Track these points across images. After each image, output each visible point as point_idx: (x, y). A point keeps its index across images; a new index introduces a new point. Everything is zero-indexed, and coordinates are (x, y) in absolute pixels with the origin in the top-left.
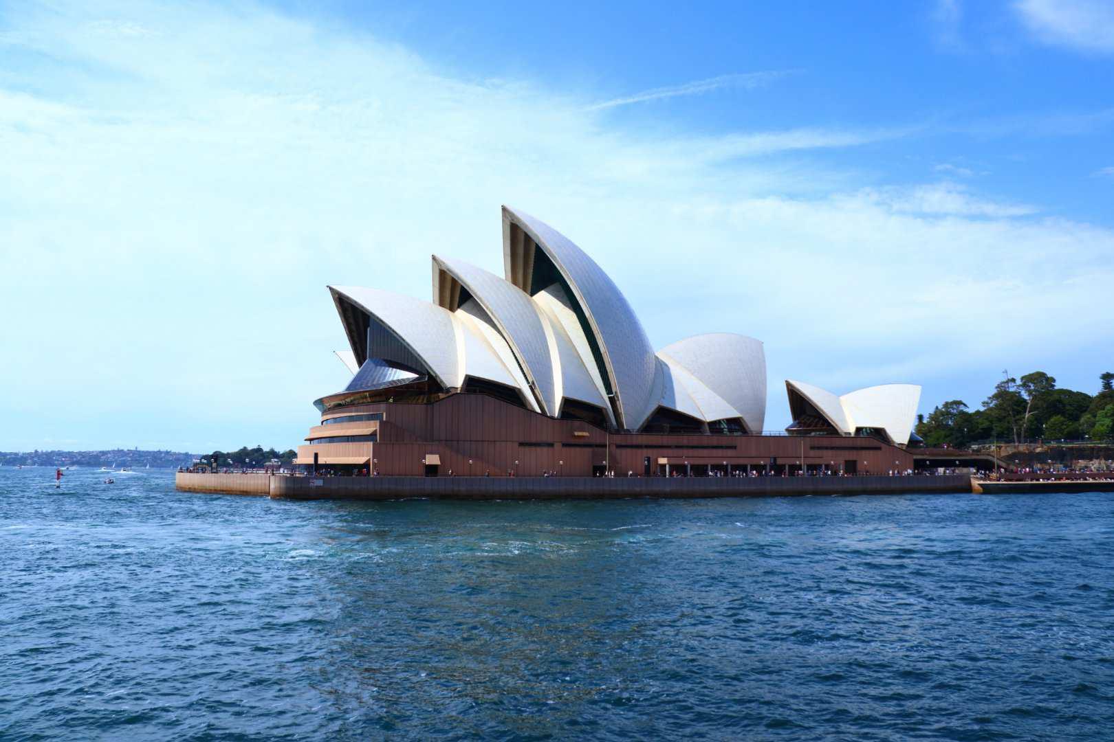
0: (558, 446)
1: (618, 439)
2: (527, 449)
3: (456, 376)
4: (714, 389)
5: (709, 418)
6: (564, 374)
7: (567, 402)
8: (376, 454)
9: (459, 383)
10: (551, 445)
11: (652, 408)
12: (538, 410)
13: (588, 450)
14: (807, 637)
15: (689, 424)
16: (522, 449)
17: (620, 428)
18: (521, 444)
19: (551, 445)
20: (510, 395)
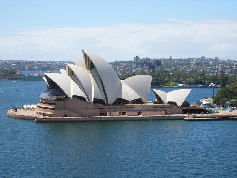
0: (92, 109)
1: (106, 107)
2: (86, 110)
3: (71, 94)
4: (135, 91)
5: (131, 100)
6: (94, 91)
7: (95, 99)
8: (55, 112)
9: (72, 97)
10: (91, 109)
11: (117, 98)
12: (88, 102)
13: (100, 109)
14: (231, 158)
15: (126, 102)
16: (85, 110)
17: (108, 104)
18: (84, 109)
19: (91, 109)
20: (82, 99)
